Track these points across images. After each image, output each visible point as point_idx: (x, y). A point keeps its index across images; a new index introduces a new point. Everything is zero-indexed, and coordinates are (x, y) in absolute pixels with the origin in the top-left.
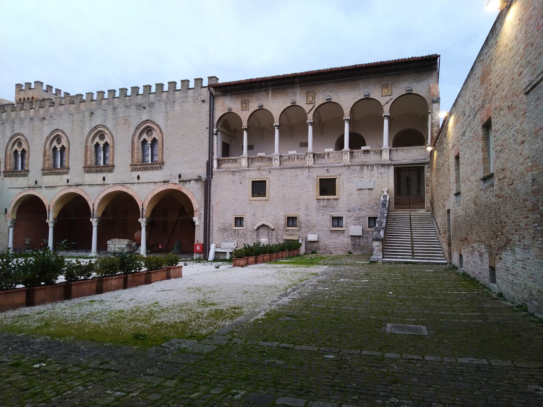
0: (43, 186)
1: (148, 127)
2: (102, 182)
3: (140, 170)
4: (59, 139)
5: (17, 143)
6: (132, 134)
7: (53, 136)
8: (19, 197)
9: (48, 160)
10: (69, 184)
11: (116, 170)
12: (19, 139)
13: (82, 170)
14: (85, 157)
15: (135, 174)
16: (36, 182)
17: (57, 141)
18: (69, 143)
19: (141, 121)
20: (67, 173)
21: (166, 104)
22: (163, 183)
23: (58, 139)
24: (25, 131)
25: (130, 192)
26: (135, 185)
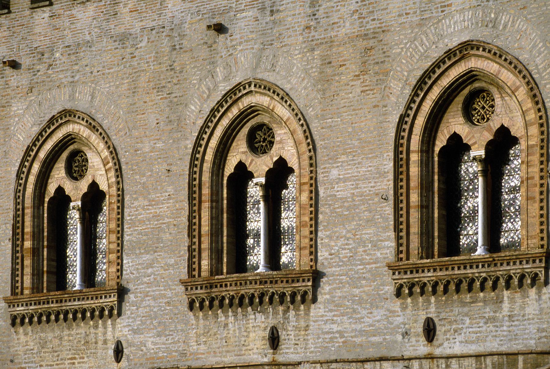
1: (470, 77)
4: (76, 153)
13: (180, 295)
14: (191, 236)
18: (119, 172)
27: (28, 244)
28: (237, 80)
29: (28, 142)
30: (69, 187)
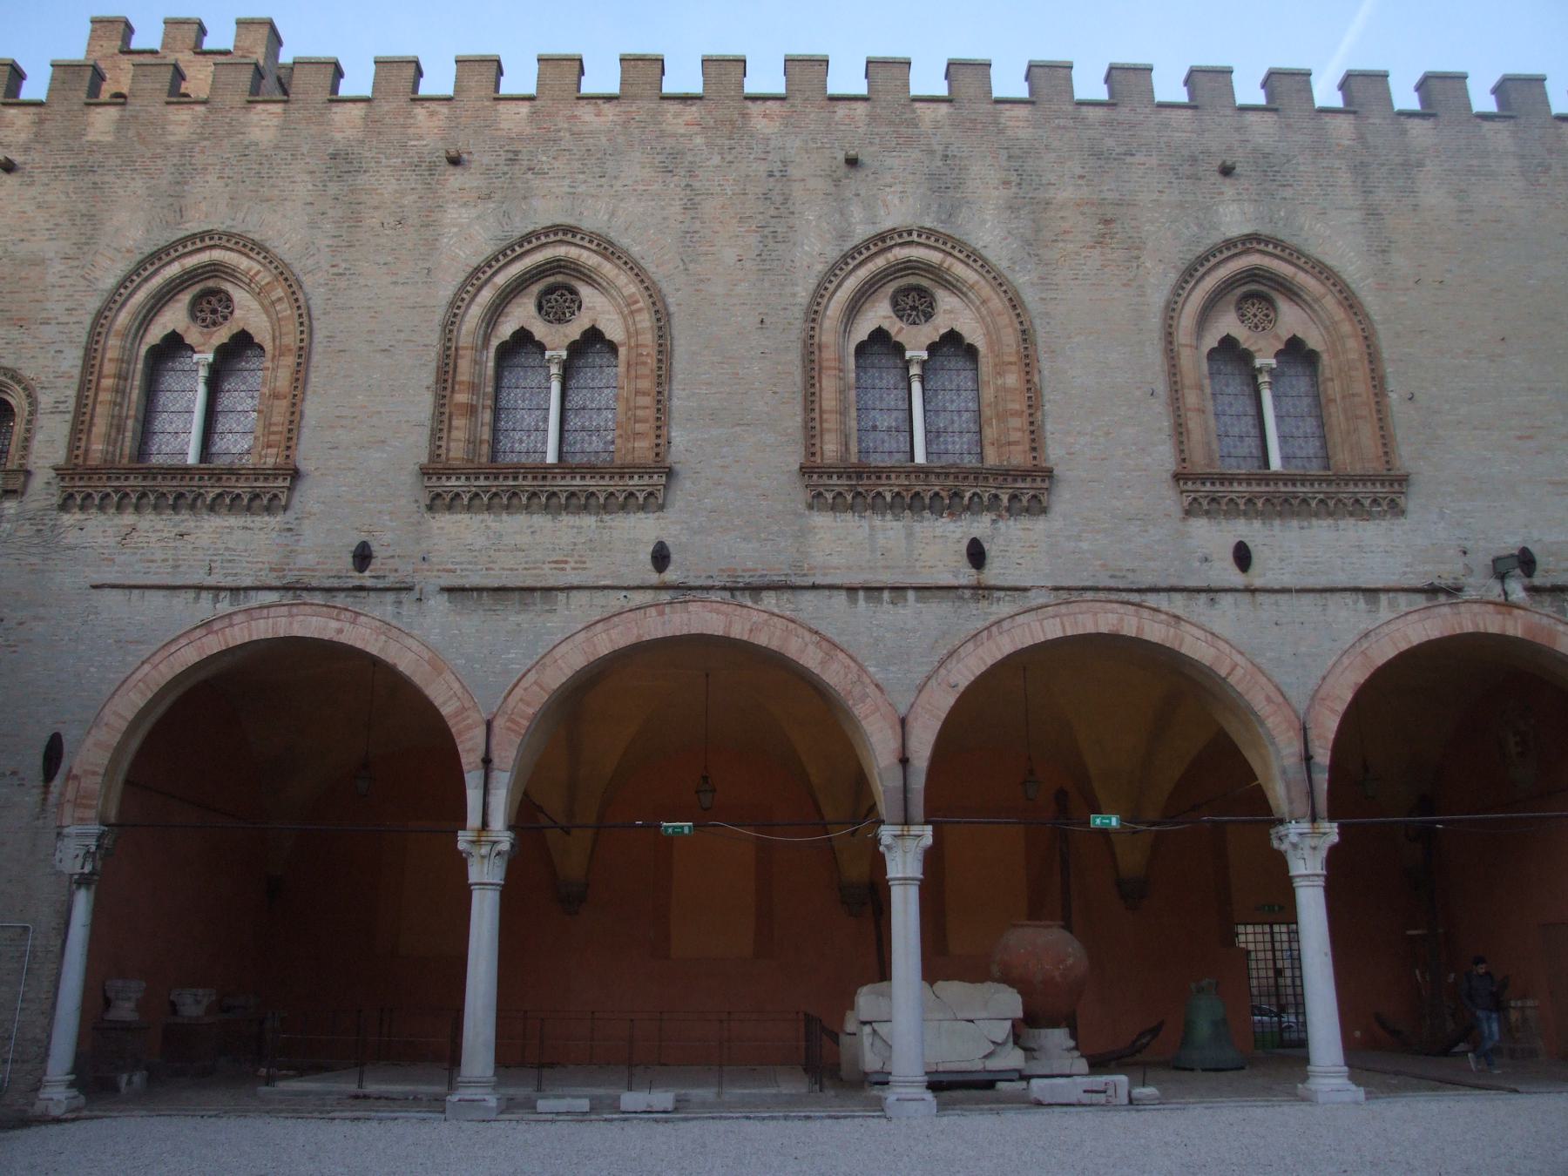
0: (432, 580)
1: (1253, 275)
2: (967, 576)
3: (1250, 509)
5: (185, 298)
6: (1157, 299)
7: (516, 269)
8: (189, 655)
9: (472, 410)
10: (671, 575)
11: (1063, 501)
12: (215, 269)
15: (1213, 538)
16: (363, 556)
17: (540, 308)
18: (662, 318)
19: (1216, 238)
20: (652, 502)
21: (1360, 169)
22: (1421, 601)
23: (557, 289)
24: (286, 228)
25: (1195, 647)
26: (1226, 600)
27: (462, 397)
28: (887, 225)
29: (475, 261)
30: (540, 330)
